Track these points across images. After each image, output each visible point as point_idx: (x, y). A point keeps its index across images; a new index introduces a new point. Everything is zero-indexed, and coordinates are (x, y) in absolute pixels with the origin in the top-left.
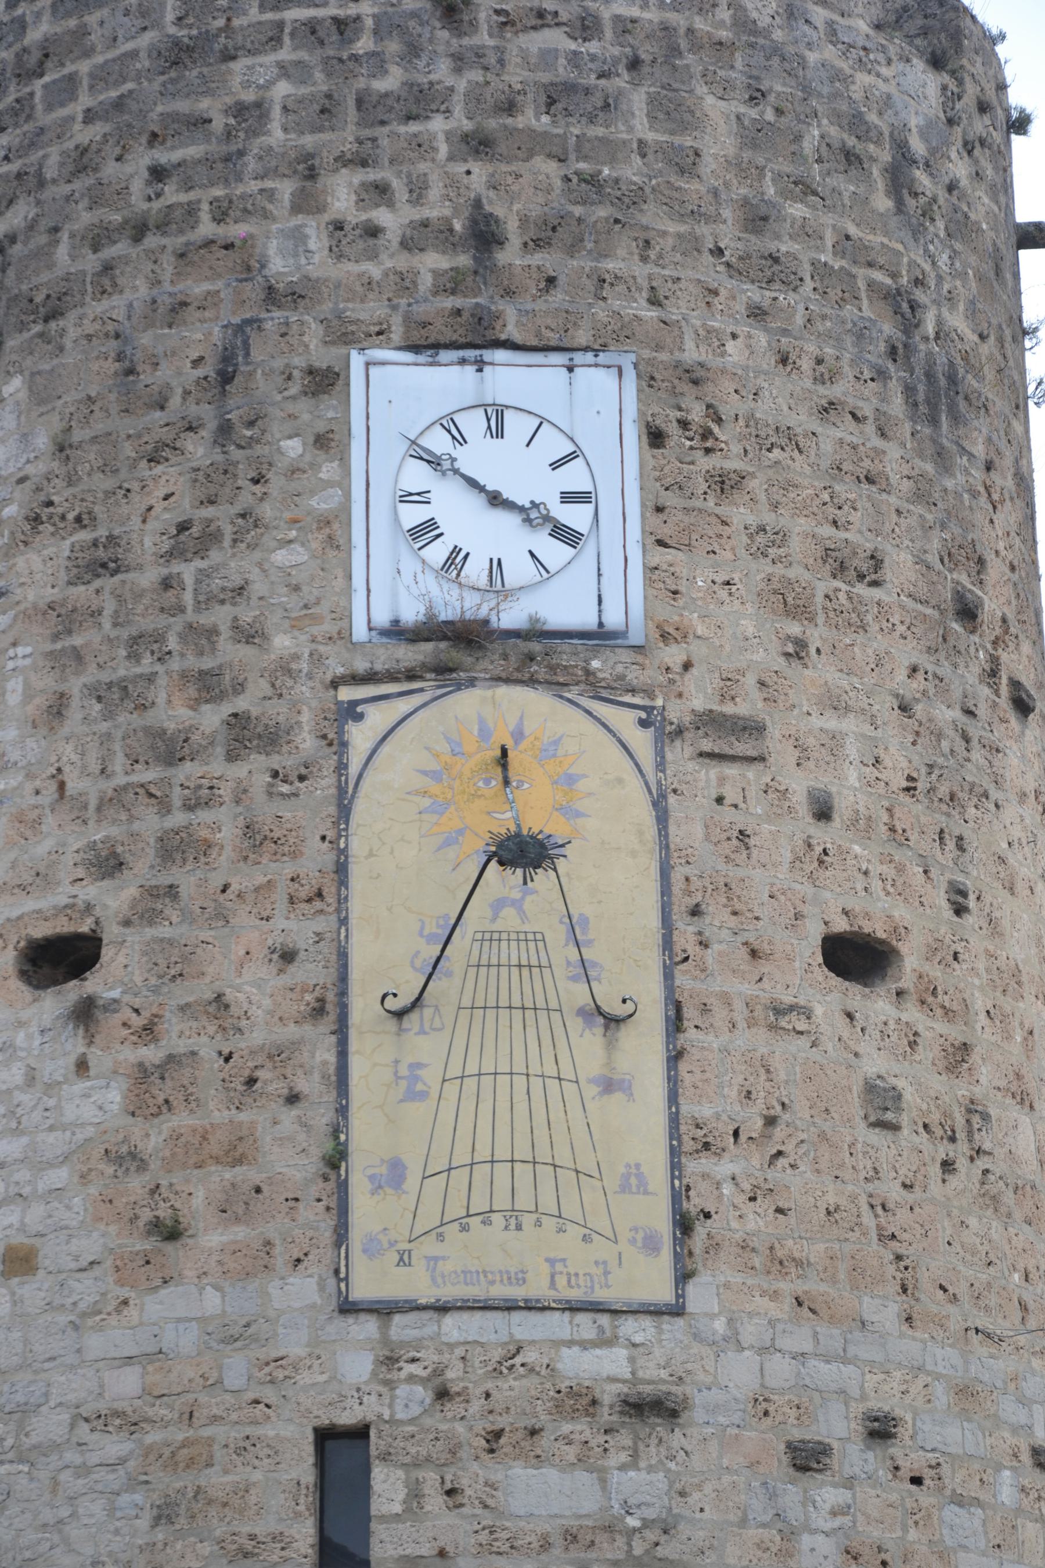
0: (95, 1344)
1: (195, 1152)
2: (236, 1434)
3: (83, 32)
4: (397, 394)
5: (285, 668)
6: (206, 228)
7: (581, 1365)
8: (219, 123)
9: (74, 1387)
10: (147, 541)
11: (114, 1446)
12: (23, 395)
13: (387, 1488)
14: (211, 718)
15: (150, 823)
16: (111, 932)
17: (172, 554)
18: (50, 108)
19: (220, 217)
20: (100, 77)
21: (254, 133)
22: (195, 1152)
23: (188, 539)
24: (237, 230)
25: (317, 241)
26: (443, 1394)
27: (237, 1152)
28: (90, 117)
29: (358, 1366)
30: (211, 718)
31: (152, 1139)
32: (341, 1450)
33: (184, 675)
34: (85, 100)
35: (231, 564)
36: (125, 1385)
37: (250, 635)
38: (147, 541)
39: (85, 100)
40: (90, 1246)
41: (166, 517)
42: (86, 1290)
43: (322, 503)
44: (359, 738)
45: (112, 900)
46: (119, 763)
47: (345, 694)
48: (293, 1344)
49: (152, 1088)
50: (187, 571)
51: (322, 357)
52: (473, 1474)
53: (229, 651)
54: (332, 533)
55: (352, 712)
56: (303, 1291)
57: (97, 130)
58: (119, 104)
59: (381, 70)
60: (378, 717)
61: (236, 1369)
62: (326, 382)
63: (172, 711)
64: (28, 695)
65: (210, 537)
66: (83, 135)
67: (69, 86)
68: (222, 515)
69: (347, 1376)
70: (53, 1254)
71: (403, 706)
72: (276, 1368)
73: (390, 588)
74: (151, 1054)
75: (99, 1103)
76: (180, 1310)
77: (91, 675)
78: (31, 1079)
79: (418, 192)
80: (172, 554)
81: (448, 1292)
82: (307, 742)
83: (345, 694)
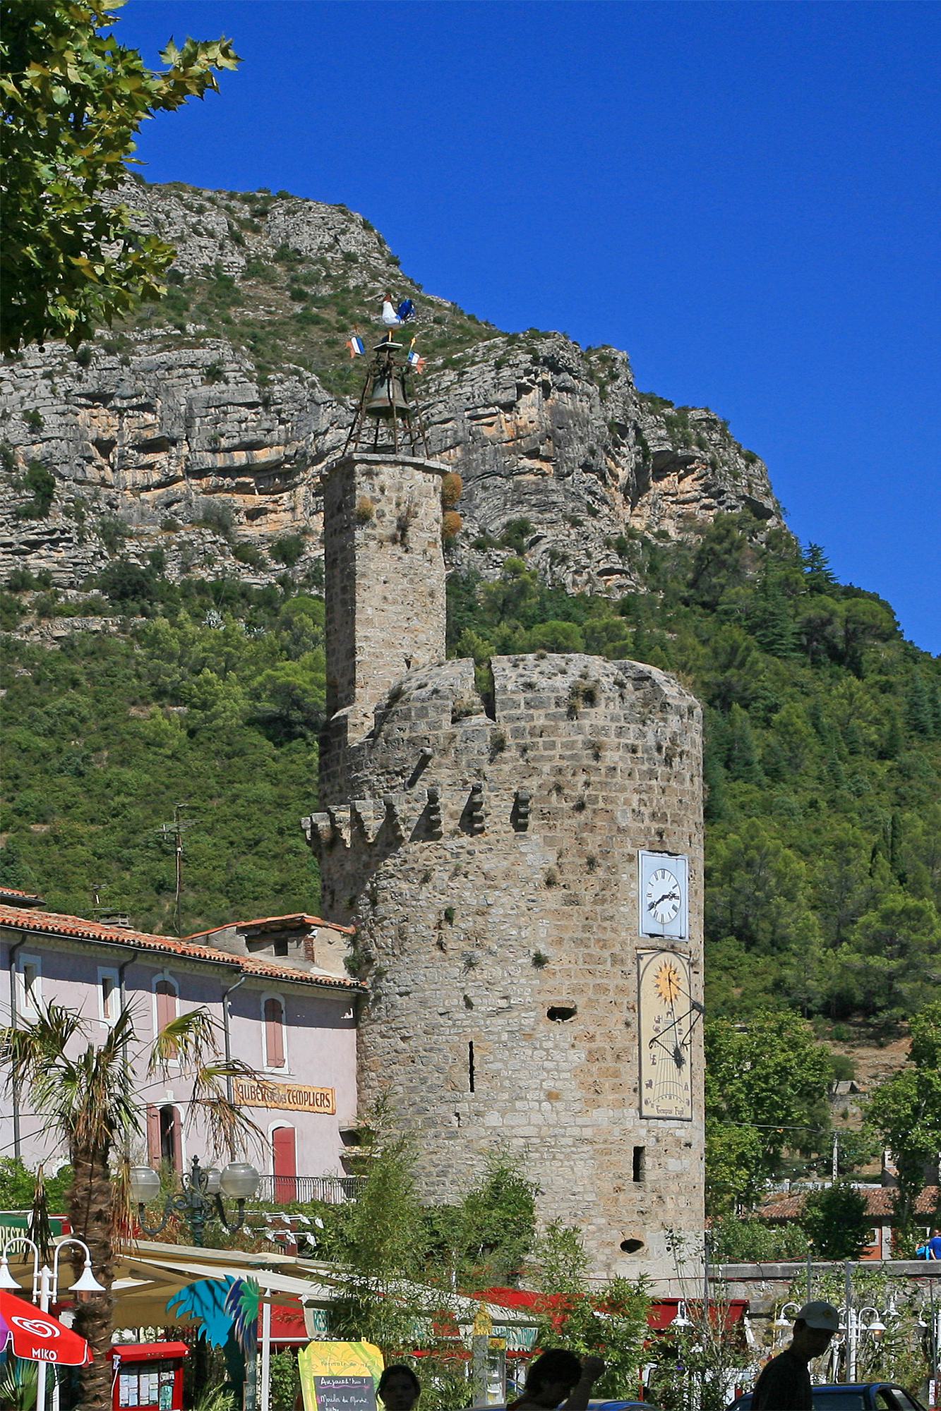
0: (580, 1121)
1: (605, 1073)
2: (617, 1148)
3: (556, 728)
4: (648, 861)
5: (623, 943)
6: (601, 805)
7: (679, 1133)
8: (603, 771)
9: (576, 1132)
10: (588, 897)
11: (585, 1148)
12: (541, 841)
13: (648, 1162)
14: (606, 954)
15: (591, 981)
16: (579, 1010)
17: (595, 903)
18: (545, 749)
19: (605, 799)
20: (564, 745)
21: (613, 777)
22: (605, 1073)
23: (599, 900)
24: (609, 807)
25: (630, 815)
26: (658, 1141)
27: (616, 1074)
28: (562, 757)
29: (643, 1132)
30: (606, 954)
31: (594, 1068)
32: (638, 1152)
33: (599, 940)
34: (558, 751)
35: (609, 909)
36: (588, 1133)
37: (614, 930)
38: (588, 897)
39: (558, 751)
40: (578, 1095)
41: (592, 892)
42: (577, 1106)
43: (632, 895)
44: (643, 964)
45: (580, 1002)
46: (581, 961)
47: (639, 952)
48: (629, 1126)
49: (593, 1057)
50: (598, 908)
51: (630, 849)
52: (662, 1160)
53: (609, 935)
54: (635, 903)
55: (639, 957)
56: (633, 1111)
57: (564, 763)
58: (573, 757)
59: (643, 763)
60: (646, 959)
61: (617, 1131)
62: (631, 858)
63: (595, 950)
64: (548, 936)
65: (604, 901)
66: (558, 763)
67: (552, 746)
68: (608, 893)
69: (641, 1136)
70: (568, 1096)
71: (651, 956)
72: (625, 1132)
73: (648, 924)
74: (593, 1045)
75: (578, 1057)
76: (601, 1116)
77: (570, 934)
78: (556, 1047)
79: (651, 801)
80: (595, 903)
81: (661, 1115)
82: (630, 966)
83: (639, 952)
